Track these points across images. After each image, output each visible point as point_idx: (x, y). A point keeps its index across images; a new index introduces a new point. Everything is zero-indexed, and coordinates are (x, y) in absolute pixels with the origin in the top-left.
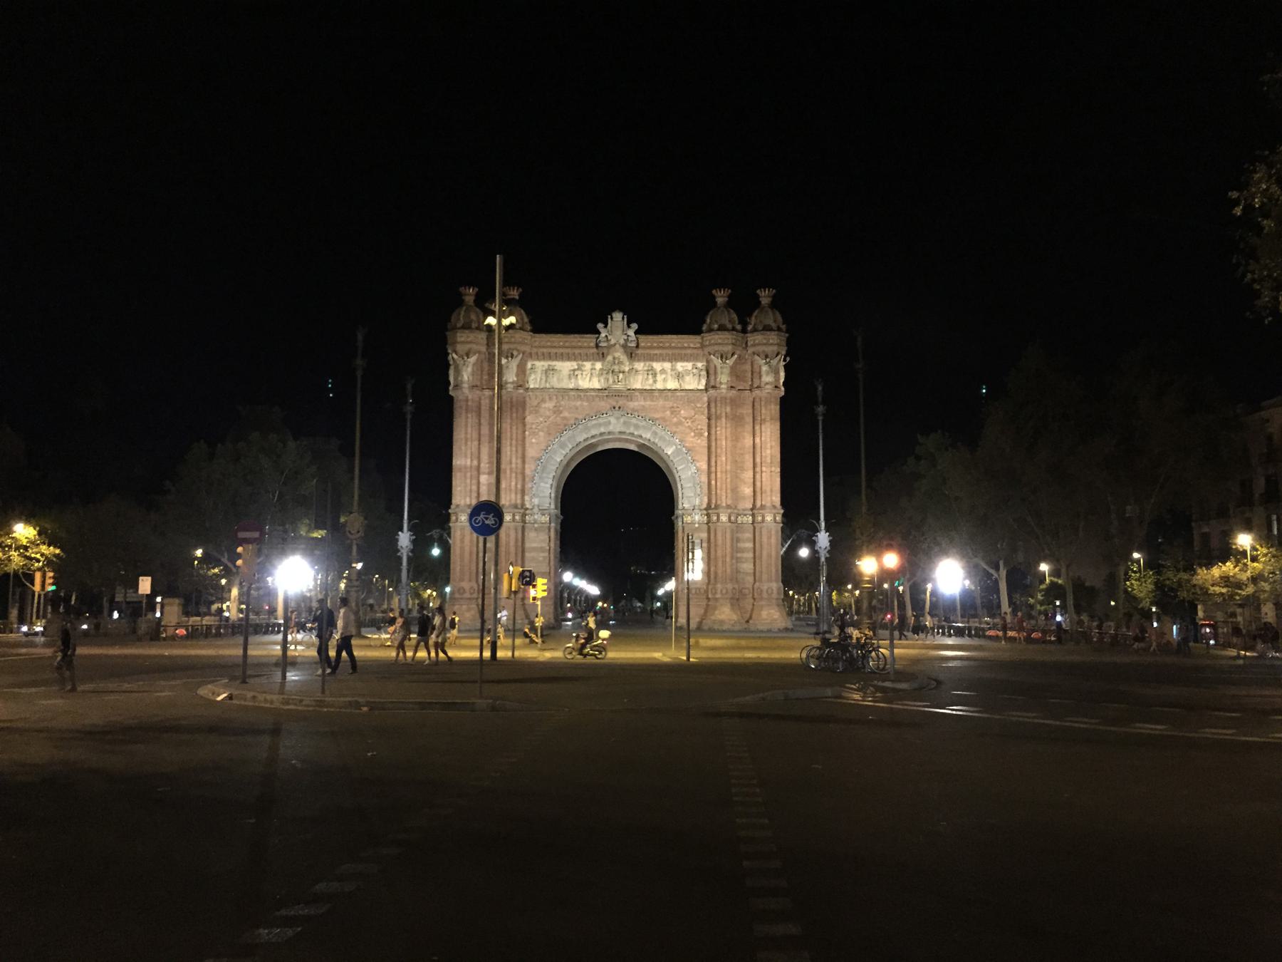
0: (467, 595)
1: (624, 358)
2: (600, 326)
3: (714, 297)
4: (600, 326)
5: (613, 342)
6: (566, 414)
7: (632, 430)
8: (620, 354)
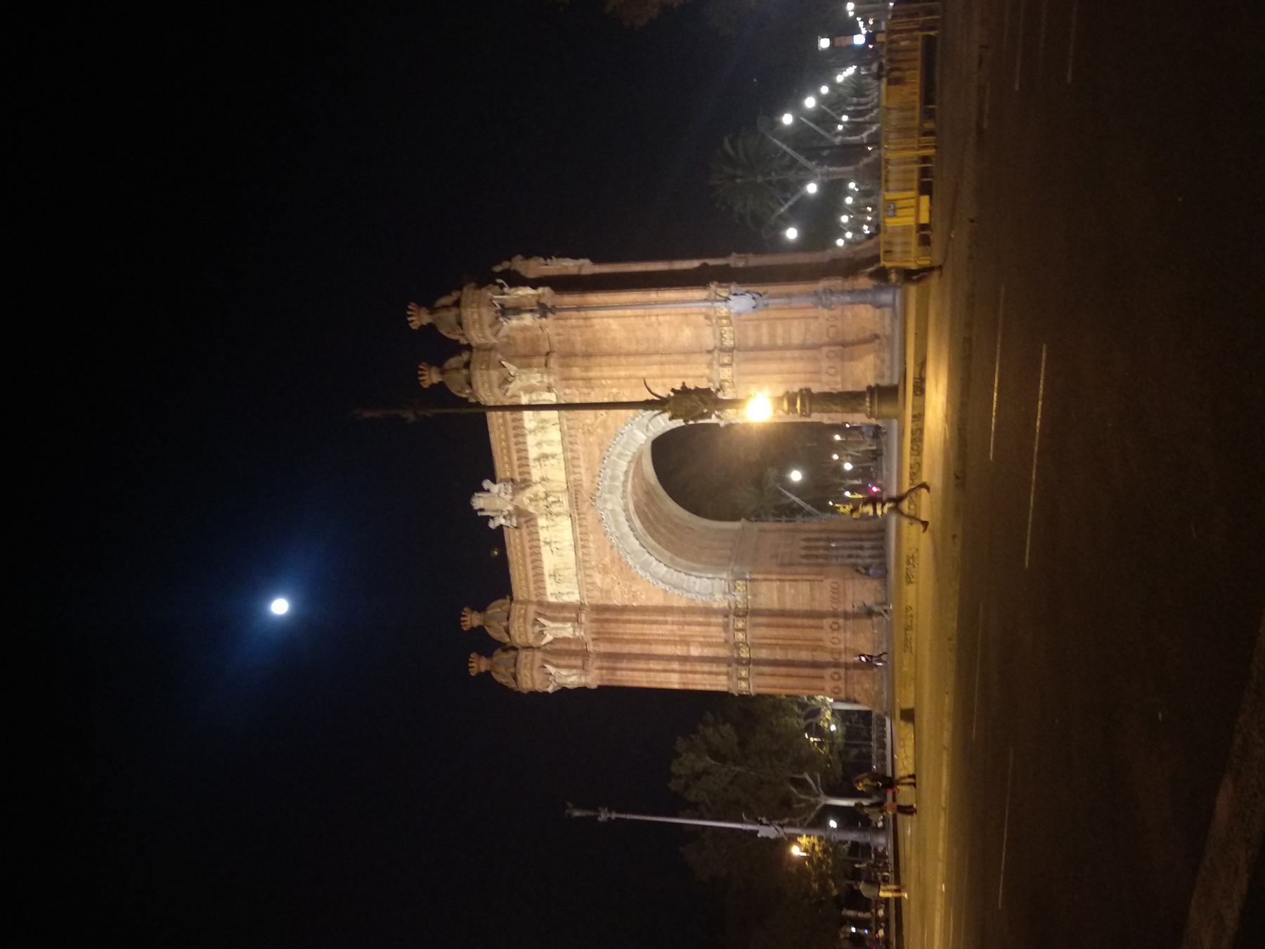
0: (841, 684)
1: (529, 493)
2: (492, 525)
3: (433, 385)
4: (492, 525)
5: (510, 508)
6: (607, 560)
7: (618, 484)
8: (524, 498)
